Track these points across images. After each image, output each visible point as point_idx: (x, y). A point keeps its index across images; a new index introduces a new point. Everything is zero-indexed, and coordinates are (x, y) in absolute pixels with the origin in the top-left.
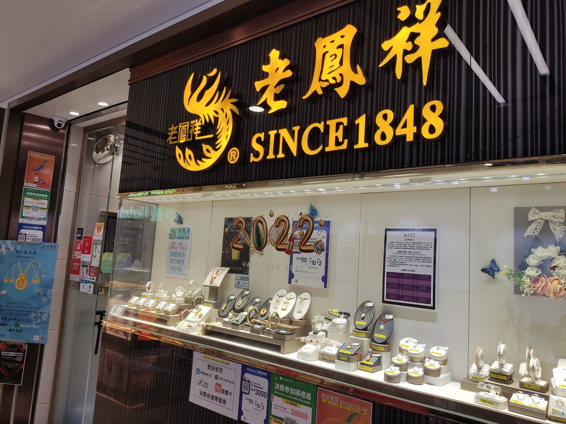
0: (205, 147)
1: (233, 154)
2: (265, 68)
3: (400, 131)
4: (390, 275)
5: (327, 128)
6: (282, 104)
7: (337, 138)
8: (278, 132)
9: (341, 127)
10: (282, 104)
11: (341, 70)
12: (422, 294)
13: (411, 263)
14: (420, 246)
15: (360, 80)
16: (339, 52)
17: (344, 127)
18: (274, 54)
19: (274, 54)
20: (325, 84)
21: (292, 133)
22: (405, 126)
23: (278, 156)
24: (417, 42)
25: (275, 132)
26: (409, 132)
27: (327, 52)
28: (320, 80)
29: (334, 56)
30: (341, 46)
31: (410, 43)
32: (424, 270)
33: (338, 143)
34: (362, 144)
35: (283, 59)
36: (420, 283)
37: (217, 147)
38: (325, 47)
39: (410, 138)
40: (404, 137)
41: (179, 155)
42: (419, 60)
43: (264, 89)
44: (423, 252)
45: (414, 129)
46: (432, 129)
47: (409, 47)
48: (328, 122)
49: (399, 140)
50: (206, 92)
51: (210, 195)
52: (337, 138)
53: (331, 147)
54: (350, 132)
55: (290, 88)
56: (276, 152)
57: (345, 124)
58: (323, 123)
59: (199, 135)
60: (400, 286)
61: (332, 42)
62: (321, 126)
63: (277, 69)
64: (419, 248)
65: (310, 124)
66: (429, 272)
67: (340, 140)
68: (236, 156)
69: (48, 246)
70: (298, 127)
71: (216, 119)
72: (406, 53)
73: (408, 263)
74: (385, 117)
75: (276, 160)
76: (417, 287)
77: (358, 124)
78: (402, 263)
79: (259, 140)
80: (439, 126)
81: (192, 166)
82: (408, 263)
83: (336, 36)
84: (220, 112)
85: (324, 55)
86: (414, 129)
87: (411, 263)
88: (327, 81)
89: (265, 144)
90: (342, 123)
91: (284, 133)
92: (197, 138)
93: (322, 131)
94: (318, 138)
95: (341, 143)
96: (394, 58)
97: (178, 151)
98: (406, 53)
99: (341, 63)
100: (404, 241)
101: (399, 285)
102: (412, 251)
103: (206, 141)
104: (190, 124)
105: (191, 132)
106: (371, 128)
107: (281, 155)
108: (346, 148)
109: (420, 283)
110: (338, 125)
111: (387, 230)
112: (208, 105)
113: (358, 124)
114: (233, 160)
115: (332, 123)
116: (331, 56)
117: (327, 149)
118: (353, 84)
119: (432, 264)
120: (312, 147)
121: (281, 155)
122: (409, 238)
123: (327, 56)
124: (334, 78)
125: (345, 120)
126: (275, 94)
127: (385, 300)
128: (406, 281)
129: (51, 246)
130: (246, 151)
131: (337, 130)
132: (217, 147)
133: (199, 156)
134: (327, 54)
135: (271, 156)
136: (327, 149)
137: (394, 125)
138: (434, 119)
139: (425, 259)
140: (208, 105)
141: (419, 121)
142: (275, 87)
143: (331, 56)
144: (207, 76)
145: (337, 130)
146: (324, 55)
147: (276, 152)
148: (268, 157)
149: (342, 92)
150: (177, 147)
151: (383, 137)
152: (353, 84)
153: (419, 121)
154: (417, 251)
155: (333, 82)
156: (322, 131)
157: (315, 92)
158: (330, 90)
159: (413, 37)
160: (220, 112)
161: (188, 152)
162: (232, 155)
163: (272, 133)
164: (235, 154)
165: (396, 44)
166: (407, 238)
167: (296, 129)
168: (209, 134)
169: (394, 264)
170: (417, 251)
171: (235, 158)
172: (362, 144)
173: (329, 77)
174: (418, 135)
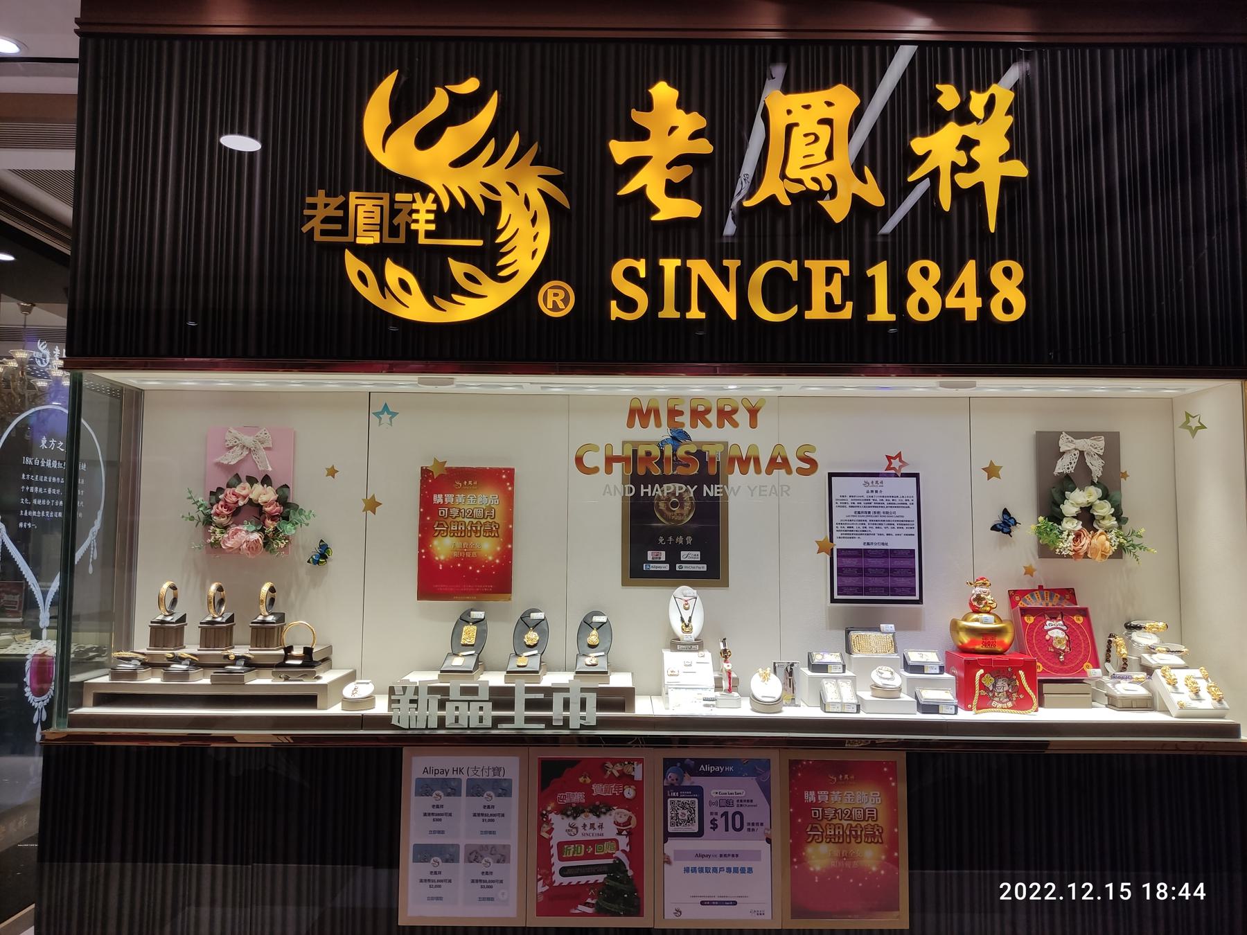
0: (458, 269)
1: (556, 295)
2: (638, 117)
3: (952, 302)
4: (843, 553)
5: (805, 274)
6: (688, 208)
7: (829, 297)
8: (684, 263)
9: (837, 278)
10: (688, 208)
11: (830, 167)
12: (902, 581)
13: (879, 531)
14: (893, 502)
15: (873, 195)
16: (824, 132)
17: (844, 279)
18: (663, 93)
19: (663, 93)
20: (796, 189)
21: (723, 274)
22: (961, 294)
23: (689, 315)
24: (976, 153)
25: (678, 262)
26: (971, 306)
27: (796, 125)
28: (783, 176)
29: (812, 138)
30: (827, 122)
31: (963, 153)
32: (902, 541)
33: (830, 305)
34: (882, 313)
35: (688, 111)
36: (898, 563)
37: (503, 273)
38: (789, 112)
39: (971, 316)
40: (961, 312)
41: (362, 276)
42: (979, 188)
43: (637, 164)
44: (899, 511)
45: (978, 302)
46: (1007, 307)
47: (962, 161)
48: (808, 264)
49: (951, 317)
50: (450, 131)
51: (451, 383)
52: (829, 297)
53: (818, 311)
54: (859, 289)
55: (706, 176)
56: (682, 303)
57: (846, 273)
58: (795, 262)
59: (429, 234)
60: (861, 572)
61: (807, 107)
62: (792, 268)
63: (673, 129)
64: (892, 505)
65: (774, 258)
66: (912, 544)
67: (837, 300)
68: (566, 301)
69: (585, 825)
70: (738, 263)
71: (494, 208)
72: (955, 169)
73: (874, 531)
74: (925, 272)
75: (683, 324)
76: (893, 570)
77: (873, 277)
78: (864, 532)
79: (630, 274)
80: (1020, 304)
81: (416, 308)
82: (874, 531)
83: (816, 98)
84: (505, 190)
85: (789, 128)
86: (978, 302)
87: (879, 531)
88: (800, 181)
89: (653, 285)
90: (838, 270)
91: (700, 268)
92: (422, 240)
93: (795, 278)
94: (785, 291)
95: (840, 308)
96: (934, 175)
97: (353, 265)
98: (955, 169)
99: (829, 154)
100: (866, 495)
101: (860, 569)
102: (881, 510)
103: (463, 254)
104: (392, 201)
105: (400, 220)
106: (899, 290)
107: (695, 313)
108: (849, 317)
109: (898, 563)
110: (830, 272)
111: (831, 475)
112: (459, 163)
113: (873, 277)
114: (555, 308)
115: (817, 267)
116: (806, 135)
117: (809, 315)
118: (857, 201)
119: (915, 531)
120: (773, 308)
121: (695, 313)
122: (874, 489)
123: (796, 132)
124: (815, 180)
125: (844, 266)
126: (669, 182)
127: (836, 597)
128: (874, 562)
129: (592, 825)
130: (595, 291)
131: (829, 281)
132: (503, 273)
133: (439, 287)
134: (795, 129)
135: (669, 311)
136: (809, 315)
137: (943, 288)
138: (1011, 294)
139: (903, 523)
140: (459, 163)
141: (986, 290)
142: (669, 166)
143: (806, 135)
144: (450, 93)
145: (829, 281)
146: (789, 128)
147: (682, 303)
148: (661, 315)
149: (837, 210)
150: (348, 254)
151: (923, 307)
152: (857, 201)
153: (986, 290)
154: (889, 510)
155: (816, 187)
156: (795, 278)
157: (772, 200)
158: (808, 201)
159: (967, 144)
160: (505, 190)
161: (394, 272)
162: (550, 299)
163: (670, 266)
164: (562, 295)
165: (939, 148)
166: (870, 489)
167: (732, 265)
168: (475, 238)
169: (849, 533)
170: (889, 510)
171: (561, 305)
172: (882, 313)
173: (806, 176)
174: (984, 311)
